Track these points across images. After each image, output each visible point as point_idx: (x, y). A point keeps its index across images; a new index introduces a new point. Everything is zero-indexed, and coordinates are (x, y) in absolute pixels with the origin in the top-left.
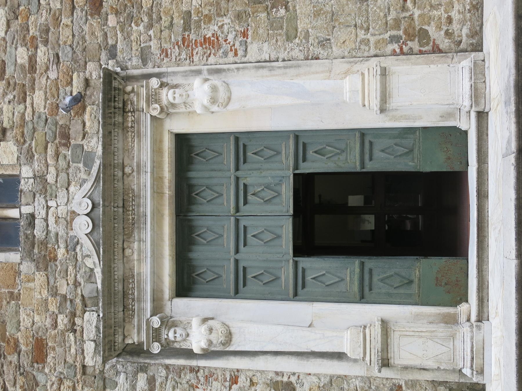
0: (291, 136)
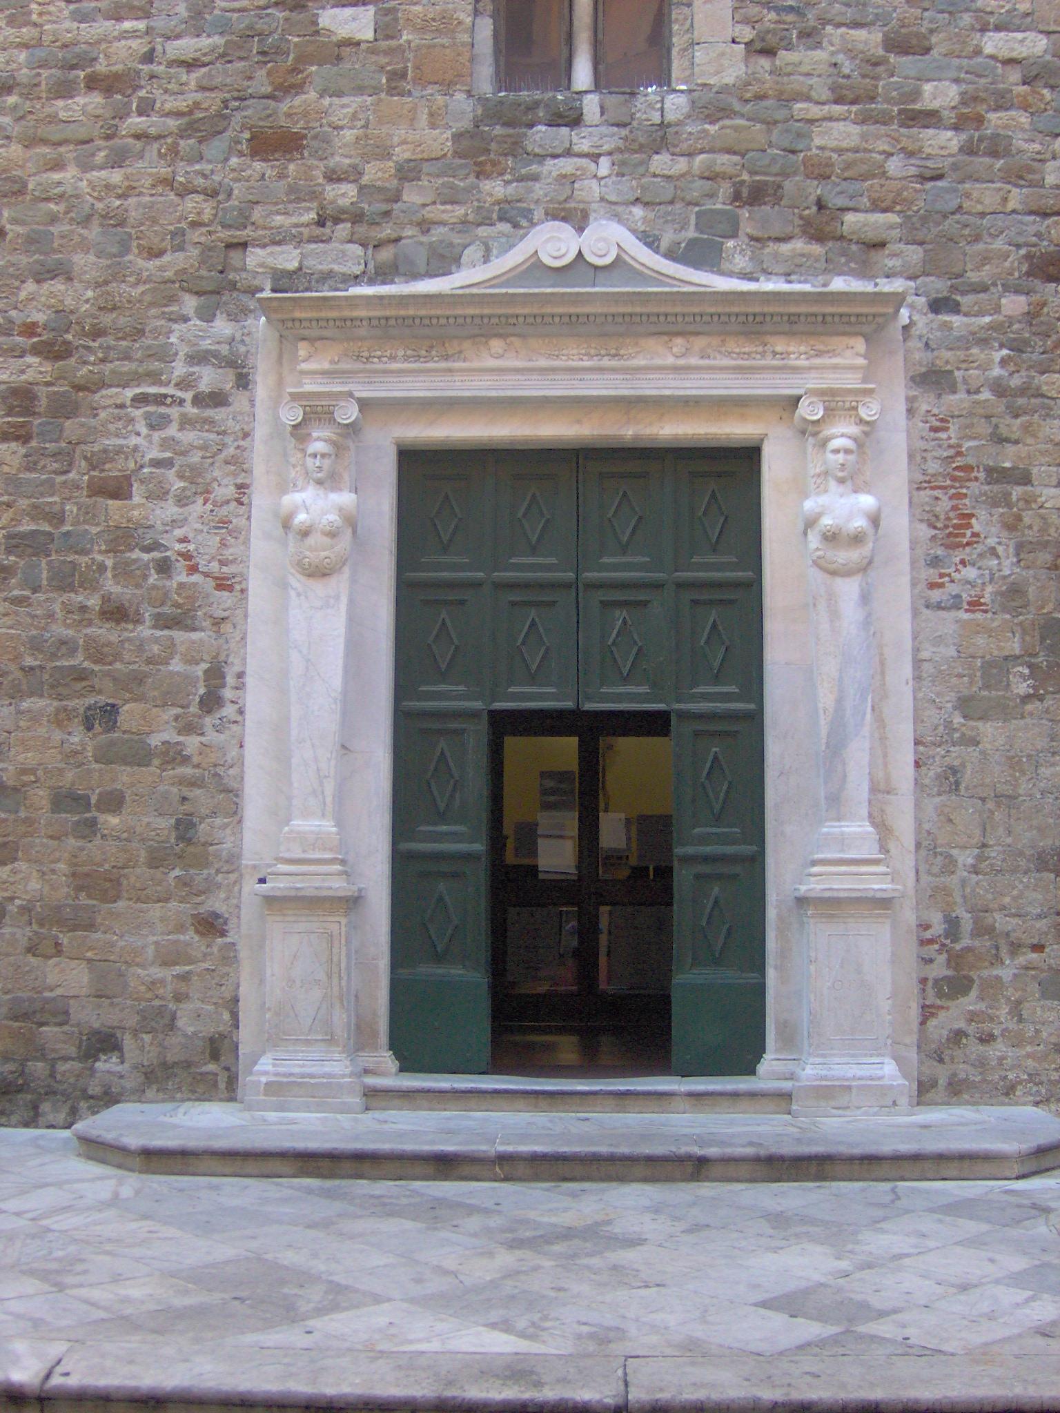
0: (752, 706)
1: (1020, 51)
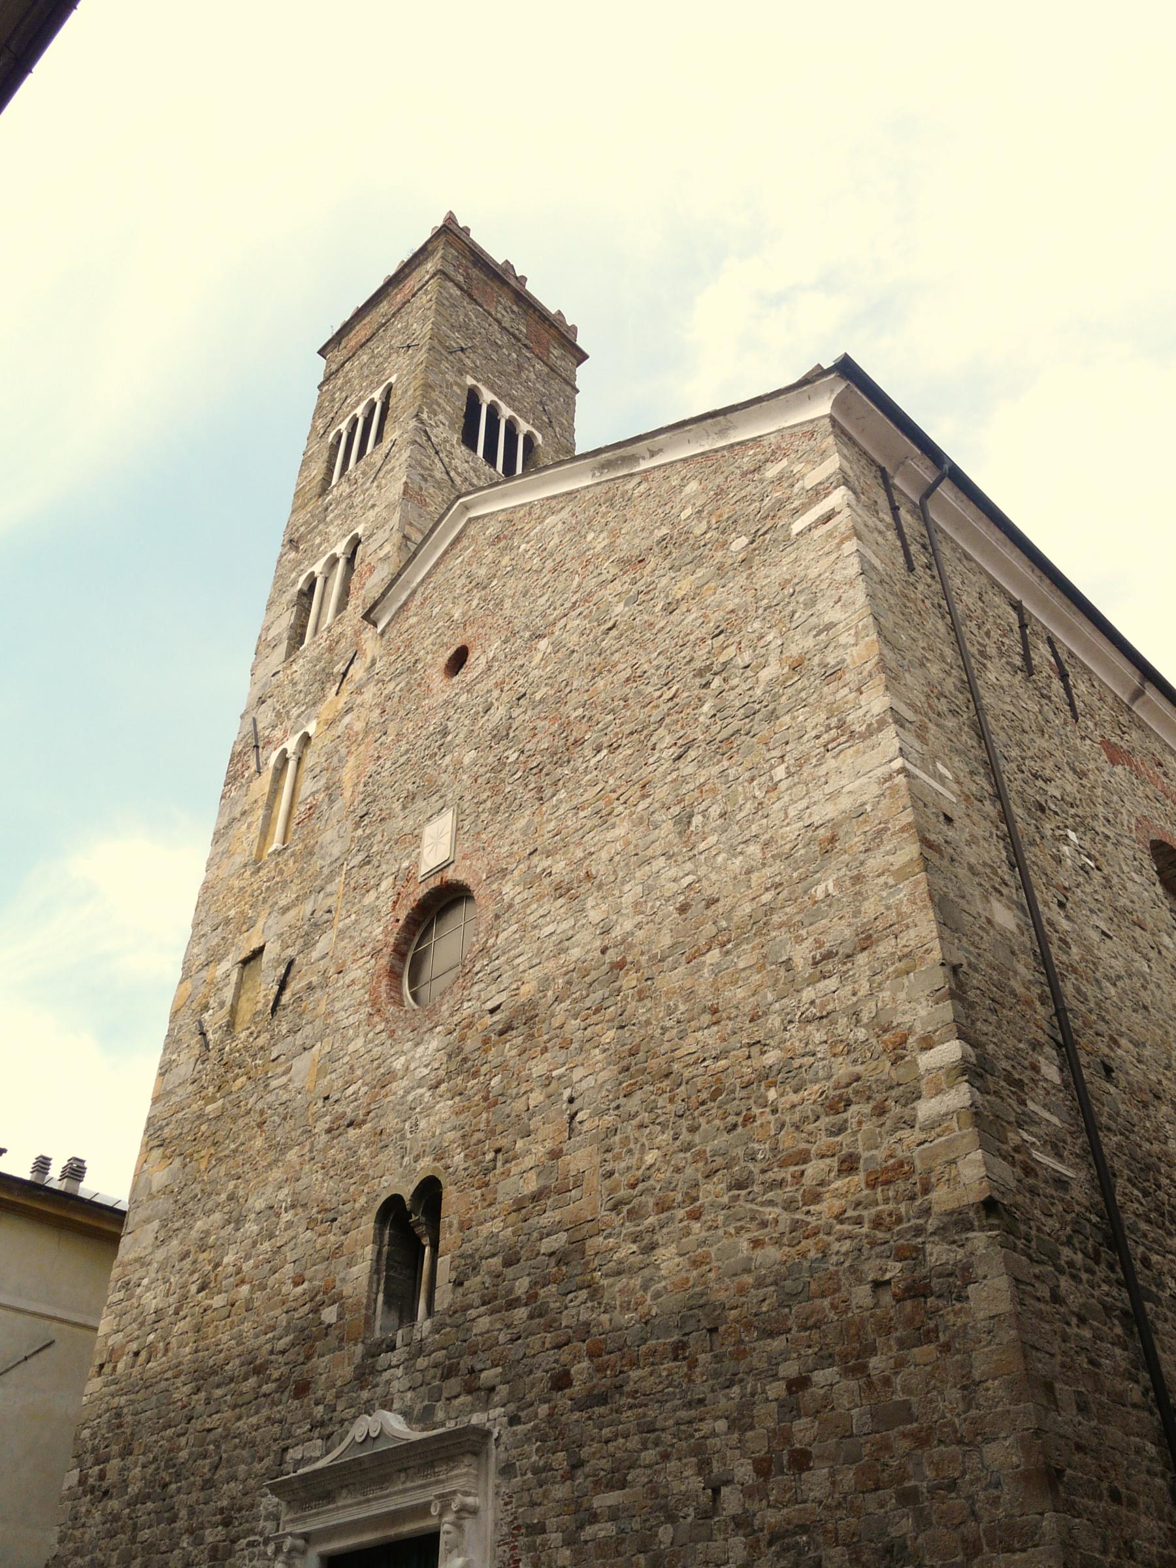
1: (556, 1246)
